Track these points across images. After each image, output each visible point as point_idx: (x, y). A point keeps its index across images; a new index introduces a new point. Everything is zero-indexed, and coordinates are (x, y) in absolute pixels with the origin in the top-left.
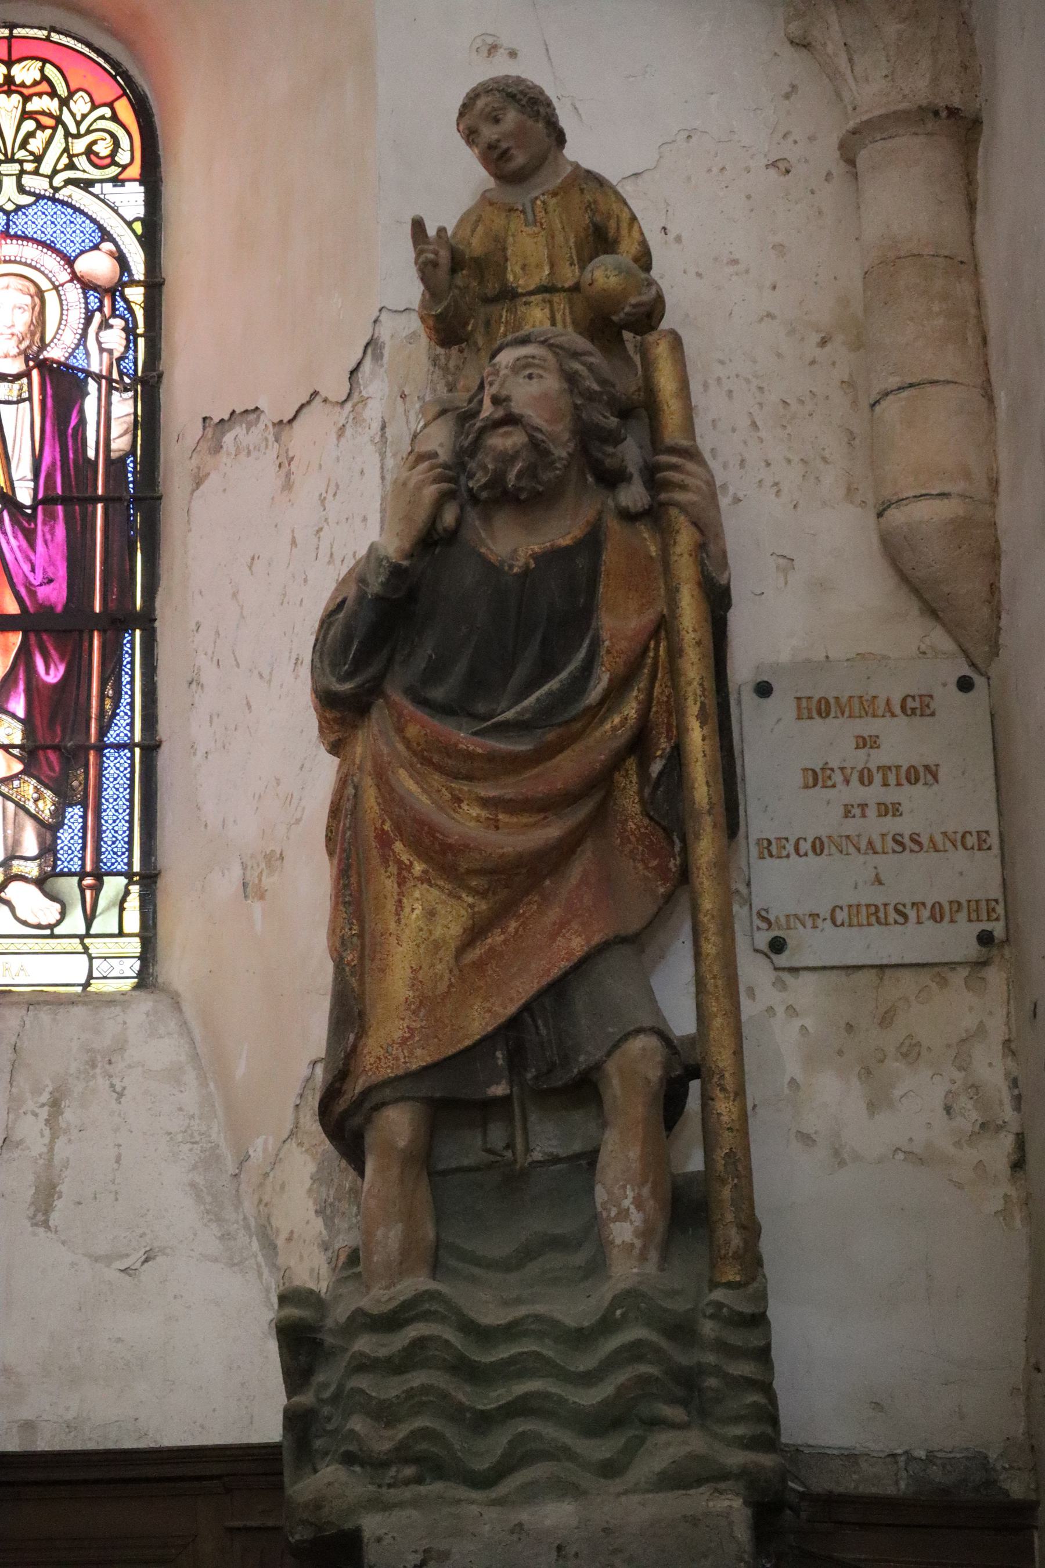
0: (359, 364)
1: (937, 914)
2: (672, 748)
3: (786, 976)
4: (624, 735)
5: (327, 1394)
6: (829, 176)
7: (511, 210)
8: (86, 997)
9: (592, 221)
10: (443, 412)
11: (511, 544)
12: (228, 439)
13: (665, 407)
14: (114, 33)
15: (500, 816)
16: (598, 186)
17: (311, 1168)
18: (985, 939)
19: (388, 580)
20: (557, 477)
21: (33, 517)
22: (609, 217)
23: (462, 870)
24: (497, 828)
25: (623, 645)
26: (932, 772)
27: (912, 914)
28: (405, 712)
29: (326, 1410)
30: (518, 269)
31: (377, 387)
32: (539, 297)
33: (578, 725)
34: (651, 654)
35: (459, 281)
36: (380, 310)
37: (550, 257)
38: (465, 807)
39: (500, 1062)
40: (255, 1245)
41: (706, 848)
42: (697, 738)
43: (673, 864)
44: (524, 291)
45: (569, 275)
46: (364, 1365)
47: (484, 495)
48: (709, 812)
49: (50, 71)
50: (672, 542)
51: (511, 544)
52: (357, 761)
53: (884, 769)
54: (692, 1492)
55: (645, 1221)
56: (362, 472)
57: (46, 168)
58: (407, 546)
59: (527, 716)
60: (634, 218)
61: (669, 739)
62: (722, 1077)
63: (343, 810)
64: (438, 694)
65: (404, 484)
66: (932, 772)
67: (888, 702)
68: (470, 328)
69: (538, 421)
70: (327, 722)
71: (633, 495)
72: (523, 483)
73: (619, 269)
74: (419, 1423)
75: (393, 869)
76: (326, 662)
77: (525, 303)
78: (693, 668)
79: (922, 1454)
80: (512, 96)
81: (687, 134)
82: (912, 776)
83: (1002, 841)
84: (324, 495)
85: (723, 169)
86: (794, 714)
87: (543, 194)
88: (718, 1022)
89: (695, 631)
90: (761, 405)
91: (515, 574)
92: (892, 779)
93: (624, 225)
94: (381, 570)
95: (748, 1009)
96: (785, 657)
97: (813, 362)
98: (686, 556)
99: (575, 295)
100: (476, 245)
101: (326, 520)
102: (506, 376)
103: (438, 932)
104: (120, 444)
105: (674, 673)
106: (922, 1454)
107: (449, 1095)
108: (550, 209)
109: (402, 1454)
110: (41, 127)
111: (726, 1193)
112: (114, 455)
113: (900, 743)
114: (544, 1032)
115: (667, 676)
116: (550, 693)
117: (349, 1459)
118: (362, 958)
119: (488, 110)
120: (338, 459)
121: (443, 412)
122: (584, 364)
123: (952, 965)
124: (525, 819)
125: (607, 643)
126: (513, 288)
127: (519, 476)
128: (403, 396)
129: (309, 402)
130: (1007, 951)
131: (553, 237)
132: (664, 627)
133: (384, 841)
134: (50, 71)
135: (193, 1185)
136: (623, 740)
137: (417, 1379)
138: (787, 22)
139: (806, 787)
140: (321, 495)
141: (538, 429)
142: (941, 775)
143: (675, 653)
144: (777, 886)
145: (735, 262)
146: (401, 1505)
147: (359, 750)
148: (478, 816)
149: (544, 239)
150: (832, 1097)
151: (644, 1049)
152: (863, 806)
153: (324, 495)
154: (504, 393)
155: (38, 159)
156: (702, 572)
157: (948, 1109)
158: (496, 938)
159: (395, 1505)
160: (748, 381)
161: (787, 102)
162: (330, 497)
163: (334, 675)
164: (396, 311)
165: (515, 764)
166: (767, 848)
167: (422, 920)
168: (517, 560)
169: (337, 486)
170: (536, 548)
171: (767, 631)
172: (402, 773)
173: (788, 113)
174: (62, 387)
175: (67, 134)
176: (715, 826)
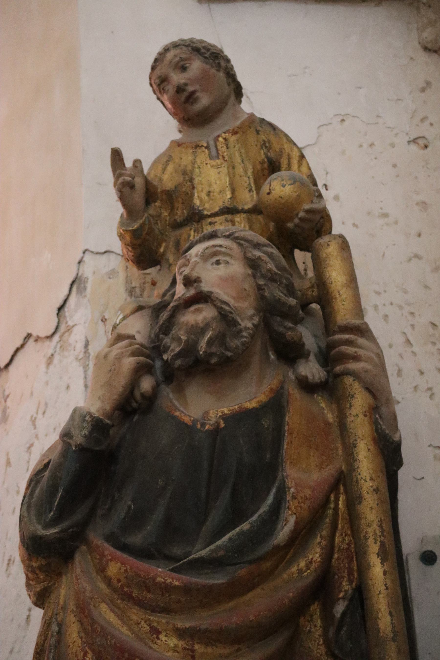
0: (65, 301)
2: (354, 590)
4: (309, 576)
7: (197, 146)
9: (267, 156)
10: (140, 308)
11: (202, 407)
13: (337, 296)
15: (197, 647)
16: (271, 129)
19: (90, 433)
20: (243, 344)
22: (281, 155)
25: (308, 492)
28: (106, 553)
30: (204, 195)
31: (80, 316)
33: (268, 564)
34: (332, 506)
35: (152, 211)
36: (84, 253)
38: (163, 637)
44: (209, 213)
45: (247, 199)
47: (178, 362)
48: (394, 640)
50: (348, 406)
51: (202, 407)
52: (61, 602)
56: (68, 387)
58: (108, 407)
59: (221, 553)
60: (302, 157)
61: (351, 582)
64: (136, 539)
65: (106, 357)
68: (162, 250)
69: (225, 298)
70: (33, 572)
71: (311, 369)
72: (214, 349)
73: (294, 181)
76: (33, 512)
81: (341, 118)
84: (35, 416)
85: (372, 145)
87: (225, 133)
89: (372, 479)
90: (413, 326)
91: (208, 430)
94: (85, 424)
98: (361, 416)
99: (254, 217)
100: (168, 180)
101: (37, 436)
102: (196, 263)
105: (353, 518)
108: (231, 144)
115: (346, 526)
119: (177, 59)
120: (47, 383)
121: (140, 308)
122: (266, 253)
125: (292, 490)
127: (210, 343)
129: (22, 346)
131: (234, 168)
132: (343, 481)
136: (310, 580)
138: (420, 30)
140: (32, 417)
141: (225, 303)
143: (353, 501)
145: (385, 215)
147: (63, 592)
148: (176, 646)
149: (226, 169)
153: (35, 416)
154: (194, 274)
156: (377, 430)
160: (400, 307)
161: (423, 94)
162: (40, 416)
163: (39, 523)
164: (97, 253)
165: (210, 597)
168: (209, 420)
169: (46, 404)
170: (226, 411)
172: (103, 607)
173: (425, 102)
176: (399, 652)
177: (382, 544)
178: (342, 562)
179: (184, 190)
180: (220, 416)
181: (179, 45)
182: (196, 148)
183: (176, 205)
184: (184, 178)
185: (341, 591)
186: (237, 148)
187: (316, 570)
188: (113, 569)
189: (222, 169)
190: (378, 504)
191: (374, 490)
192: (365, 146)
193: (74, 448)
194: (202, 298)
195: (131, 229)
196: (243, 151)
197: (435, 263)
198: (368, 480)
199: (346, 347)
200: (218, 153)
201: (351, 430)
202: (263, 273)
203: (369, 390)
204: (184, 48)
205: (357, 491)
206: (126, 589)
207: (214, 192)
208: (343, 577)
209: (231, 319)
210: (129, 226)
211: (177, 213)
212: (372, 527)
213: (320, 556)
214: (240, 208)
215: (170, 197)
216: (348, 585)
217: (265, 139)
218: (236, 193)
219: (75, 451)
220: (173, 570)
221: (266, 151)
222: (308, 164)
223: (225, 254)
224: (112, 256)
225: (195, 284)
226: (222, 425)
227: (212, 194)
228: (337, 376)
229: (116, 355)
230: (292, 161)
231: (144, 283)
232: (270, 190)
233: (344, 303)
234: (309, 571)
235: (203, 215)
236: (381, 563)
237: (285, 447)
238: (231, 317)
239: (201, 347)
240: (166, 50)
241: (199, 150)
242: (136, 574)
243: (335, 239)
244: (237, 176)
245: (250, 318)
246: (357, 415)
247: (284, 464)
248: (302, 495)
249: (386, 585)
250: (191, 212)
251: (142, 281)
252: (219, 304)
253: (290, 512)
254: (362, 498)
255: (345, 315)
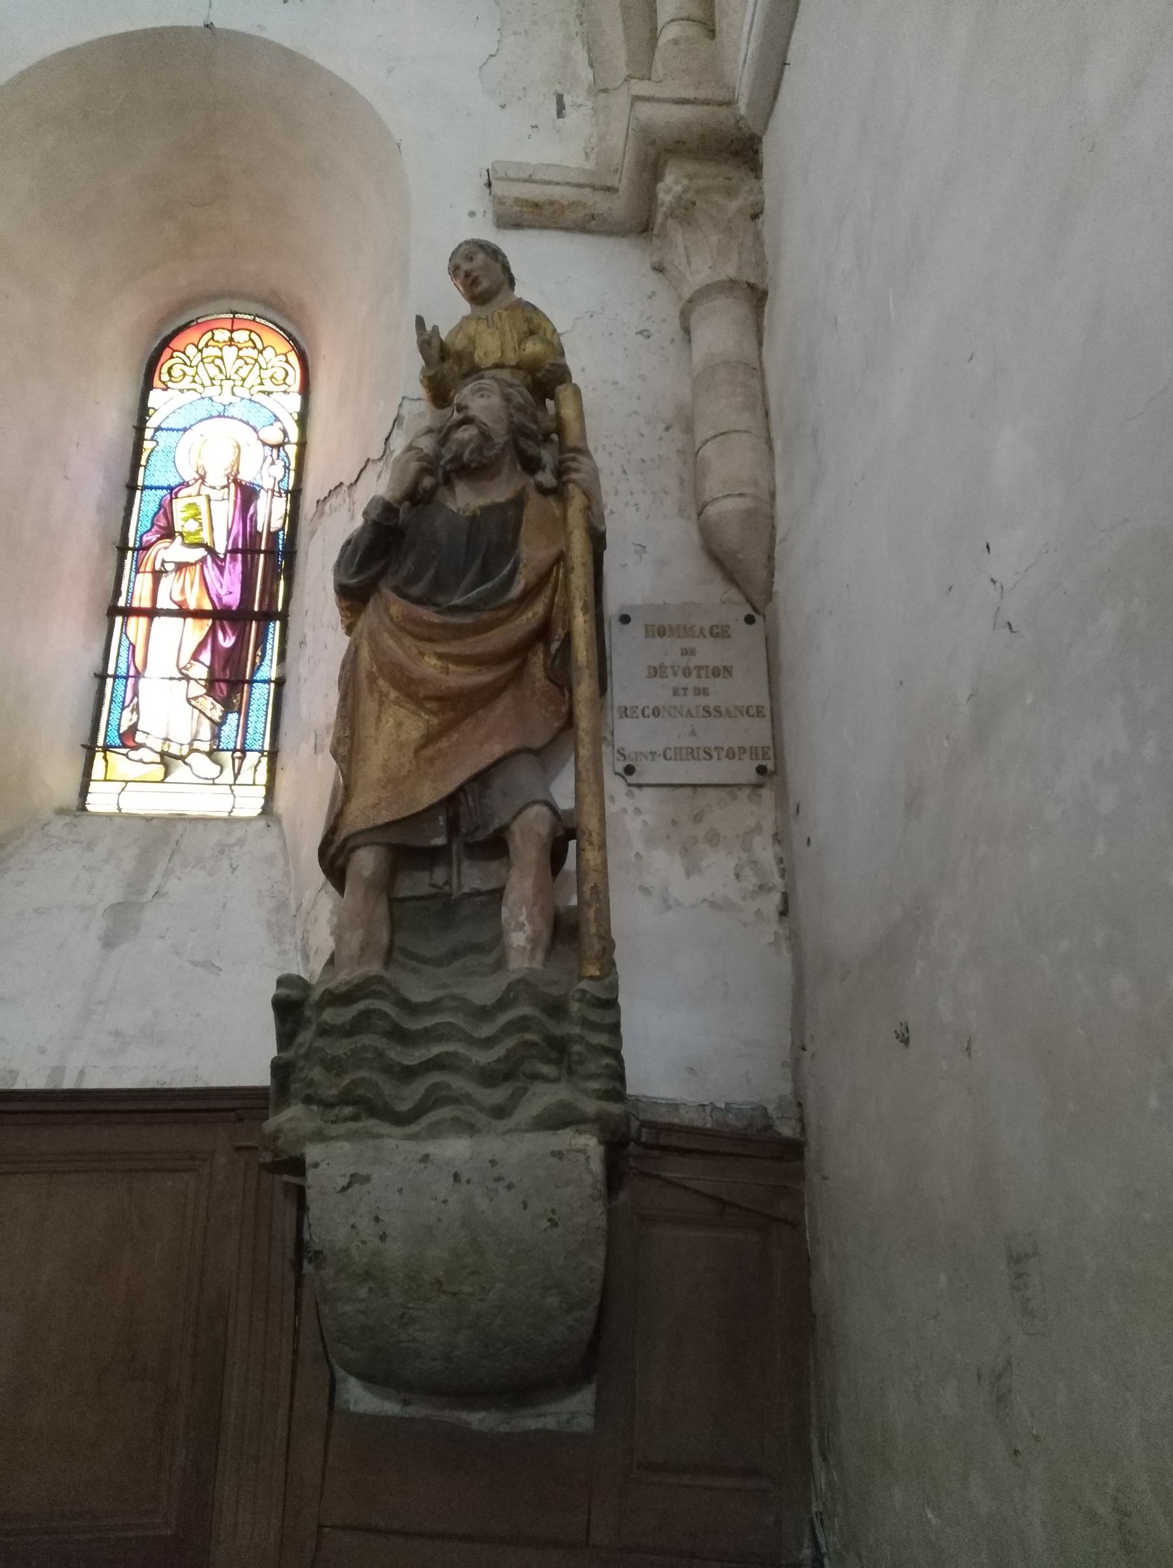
1: (731, 754)
3: (635, 790)
4: (534, 624)
5: (302, 1051)
6: (673, 341)
8: (230, 821)
11: (465, 499)
12: (327, 507)
14: (289, 318)
17: (331, 906)
18: (761, 770)
21: (224, 560)
23: (421, 696)
24: (447, 673)
26: (728, 671)
27: (715, 755)
29: (301, 1063)
33: (503, 613)
35: (446, 365)
38: (426, 658)
39: (441, 823)
40: (299, 958)
41: (584, 689)
42: (581, 622)
43: (564, 709)
45: (512, 358)
46: (325, 1031)
49: (254, 336)
51: (465, 499)
53: (699, 668)
54: (560, 1132)
55: (534, 932)
57: (247, 384)
62: (590, 835)
63: (350, 663)
66: (728, 671)
67: (702, 629)
69: (485, 420)
71: (546, 478)
72: (474, 457)
74: (363, 1073)
75: (377, 696)
78: (579, 580)
79: (723, 1106)
82: (716, 673)
83: (772, 713)
85: (611, 334)
86: (643, 634)
88: (588, 800)
90: (629, 461)
92: (703, 673)
95: (610, 808)
96: (639, 602)
97: (660, 439)
99: (516, 371)
100: (459, 344)
103: (403, 737)
104: (276, 524)
106: (723, 1106)
107: (408, 847)
109: (345, 1098)
110: (247, 364)
111: (591, 913)
112: (272, 530)
113: (708, 652)
114: (471, 804)
116: (486, 590)
117: (308, 1100)
118: (350, 751)
123: (740, 786)
124: (467, 669)
130: (775, 778)
132: (561, 558)
133: (372, 679)
134: (254, 336)
135: (268, 921)
136: (535, 625)
137: (365, 1039)
138: (651, 255)
139: (650, 677)
142: (734, 674)
143: (568, 571)
144: (629, 735)
145: (615, 383)
146: (337, 1138)
150: (664, 865)
151: (538, 814)
152: (685, 689)
154: (464, 403)
155: (244, 380)
157: (737, 876)
158: (444, 743)
159: (331, 1138)
160: (622, 448)
165: (460, 632)
166: (625, 712)
167: (395, 728)
171: (629, 582)
172: (385, 635)
174: (247, 495)
175: (261, 368)
177: (585, 602)
194: (468, 421)
203: (587, 494)
215: (460, 356)
226: (478, 513)
240: (460, 245)
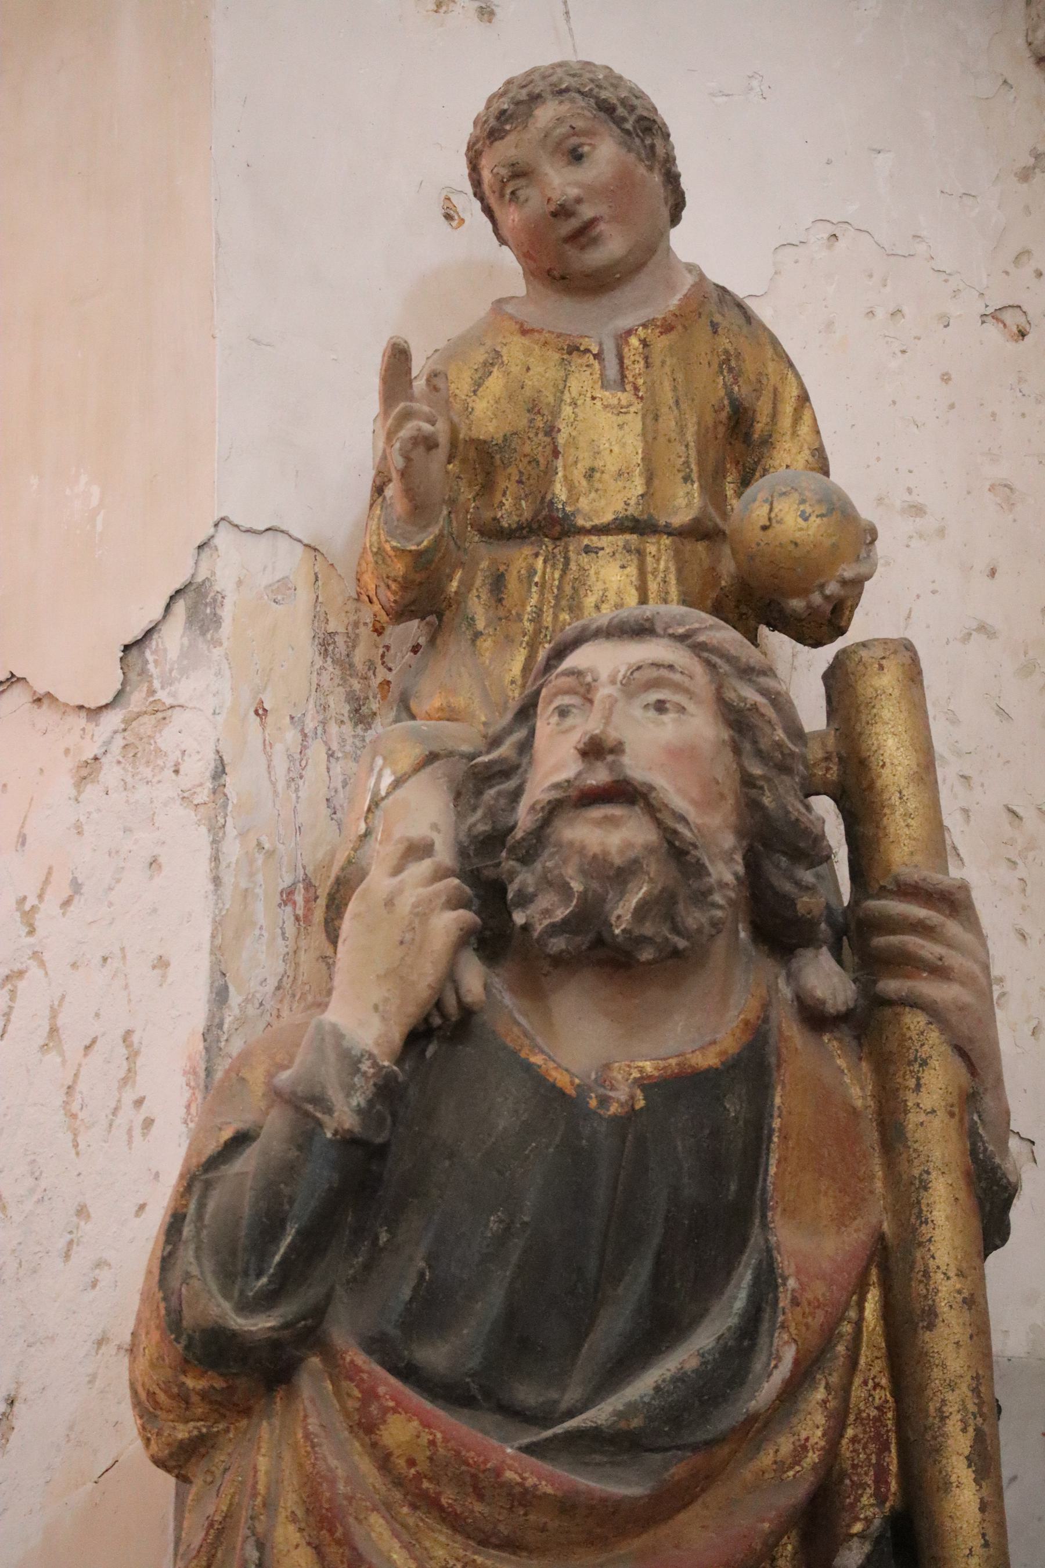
0: (149, 633)
7: (574, 349)
9: (730, 394)
10: (432, 758)
11: (594, 1049)
13: (895, 799)
16: (742, 321)
19: (371, 1103)
28: (381, 1390)
32: (620, 539)
36: (216, 525)
37: (647, 459)
44: (588, 525)
50: (912, 1083)
51: (594, 1049)
52: (261, 1488)
59: (636, 1423)
61: (881, 1498)
64: (435, 1355)
69: (679, 803)
72: (648, 929)
77: (588, 550)
80: (606, 108)
81: (830, 229)
89: (960, 1274)
91: (615, 1118)
93: (788, 409)
98: (941, 1114)
102: (613, 702)
108: (656, 359)
115: (879, 1365)
119: (563, 129)
125: (792, 1283)
126: (566, 516)
127: (641, 912)
128: (261, 712)
131: (656, 418)
141: (683, 819)
145: (917, 510)
156: (973, 1153)
163: (227, 1296)
170: (648, 1066)
172: (377, 1521)
173: (1027, 210)
178: (864, 1449)
179: (527, 449)
180: (636, 1080)
181: (567, 90)
182: (570, 353)
183: (502, 483)
184: (531, 421)
185: (857, 1519)
186: (667, 369)
187: (814, 1467)
188: (398, 1432)
189: (629, 417)
190: (971, 1337)
191: (964, 1301)
192: (881, 313)
193: (329, 1135)
195: (414, 548)
196: (680, 376)
197: (1026, 653)
198: (951, 1274)
199: (919, 941)
200: (623, 376)
201: (916, 1146)
202: (762, 747)
204: (581, 102)
205: (926, 1297)
206: (426, 1484)
207: (603, 472)
208: (864, 1486)
209: (693, 861)
210: (409, 540)
211: (502, 504)
212: (957, 1392)
213: (824, 1435)
214: (662, 522)
216: (872, 1505)
217: (729, 347)
218: (656, 482)
219: (330, 1140)
220: (529, 1449)
221: (729, 379)
222: (815, 419)
223: (677, 687)
224: (283, 542)
225: (610, 758)
227: (597, 475)
228: (883, 1002)
229: (415, 906)
230: (780, 407)
231: (356, 625)
232: (770, 519)
233: (909, 821)
234: (798, 1468)
235: (575, 526)
236: (975, 1480)
237: (773, 1170)
238: (695, 856)
239: (619, 917)
241: (577, 360)
242: (458, 1453)
243: (895, 652)
244: (662, 440)
245: (729, 860)
246: (933, 1111)
247: (770, 1214)
248: (809, 1296)
249: (984, 1535)
250: (544, 513)
251: (353, 618)
252: (671, 823)
253: (786, 1337)
254: (936, 1316)
255: (912, 853)
